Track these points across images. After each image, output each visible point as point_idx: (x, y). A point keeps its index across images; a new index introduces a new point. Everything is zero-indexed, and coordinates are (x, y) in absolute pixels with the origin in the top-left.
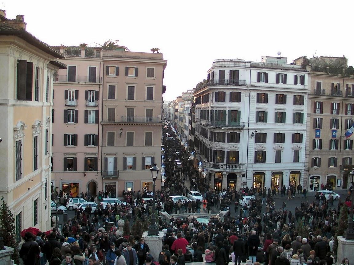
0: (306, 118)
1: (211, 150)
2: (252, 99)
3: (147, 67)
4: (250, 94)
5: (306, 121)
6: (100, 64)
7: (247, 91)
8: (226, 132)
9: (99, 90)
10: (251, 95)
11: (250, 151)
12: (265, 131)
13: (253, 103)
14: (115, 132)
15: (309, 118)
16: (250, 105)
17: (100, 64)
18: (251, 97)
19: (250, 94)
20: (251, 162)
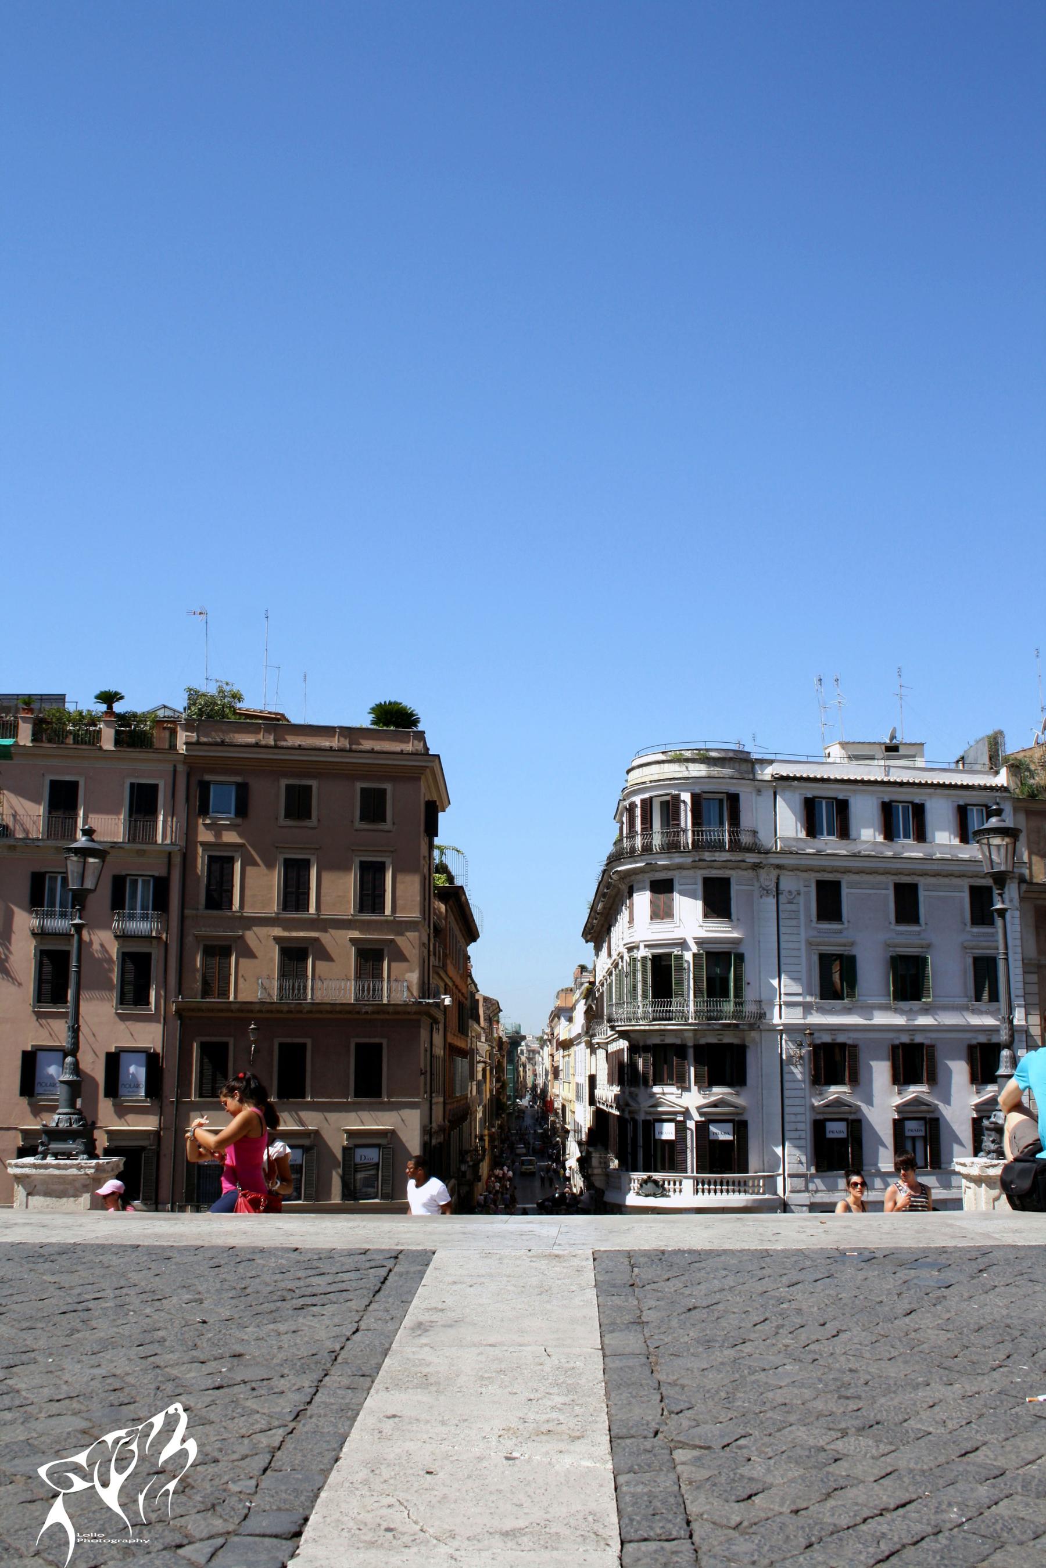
0: (1020, 978)
1: (635, 1121)
2: (789, 907)
3: (359, 785)
4: (777, 884)
5: (1021, 992)
6: (175, 771)
7: (763, 873)
8: (690, 1043)
9: (169, 873)
10: (782, 887)
11: (793, 1118)
12: (853, 1035)
13: (794, 922)
14: (231, 1041)
15: (1034, 978)
16: (782, 930)
17: (175, 771)
18: (781, 897)
19: (777, 884)
20: (803, 1169)
